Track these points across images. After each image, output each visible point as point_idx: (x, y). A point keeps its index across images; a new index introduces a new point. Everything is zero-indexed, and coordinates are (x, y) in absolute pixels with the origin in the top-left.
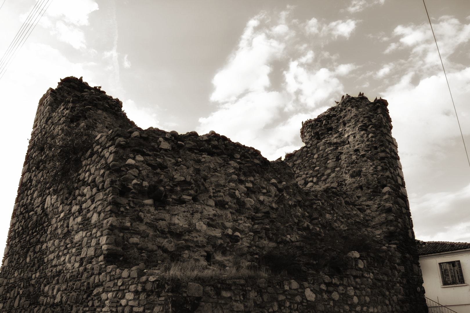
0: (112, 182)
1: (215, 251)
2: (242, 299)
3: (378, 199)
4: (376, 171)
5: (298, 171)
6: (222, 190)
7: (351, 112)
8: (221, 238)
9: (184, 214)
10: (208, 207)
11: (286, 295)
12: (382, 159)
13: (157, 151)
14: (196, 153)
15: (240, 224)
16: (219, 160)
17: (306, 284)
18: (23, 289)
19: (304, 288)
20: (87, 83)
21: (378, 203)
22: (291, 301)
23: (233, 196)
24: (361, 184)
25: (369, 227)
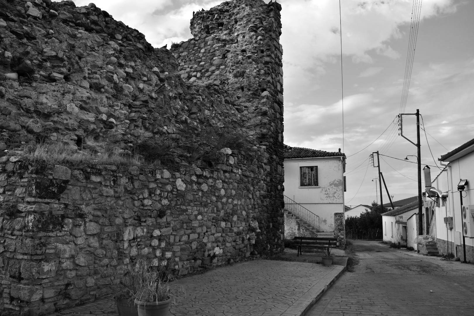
2: (113, 184)
3: (256, 101)
4: (259, 74)
5: (183, 64)
6: (98, 72)
7: (244, 11)
8: (94, 123)
9: (54, 93)
10: (82, 89)
11: (157, 183)
12: (267, 63)
13: (24, 18)
14: (71, 26)
15: (115, 110)
16: (98, 38)
17: (178, 174)
19: (176, 178)
21: (256, 105)
22: (162, 189)
23: (110, 80)
24: (242, 85)
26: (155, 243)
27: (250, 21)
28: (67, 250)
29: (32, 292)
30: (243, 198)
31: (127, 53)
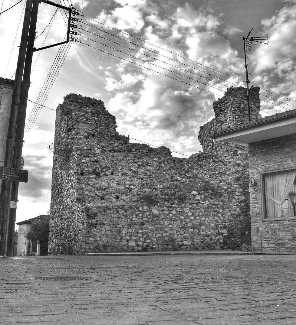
0: (77, 170)
1: (122, 195)
3: (235, 158)
8: (124, 189)
14: (113, 152)
15: (133, 182)
16: (123, 154)
17: (153, 207)
20: (80, 95)
23: (130, 170)
26: (140, 235)
27: (232, 107)
28: (98, 234)
29: (86, 245)
30: (211, 216)
31: (138, 156)
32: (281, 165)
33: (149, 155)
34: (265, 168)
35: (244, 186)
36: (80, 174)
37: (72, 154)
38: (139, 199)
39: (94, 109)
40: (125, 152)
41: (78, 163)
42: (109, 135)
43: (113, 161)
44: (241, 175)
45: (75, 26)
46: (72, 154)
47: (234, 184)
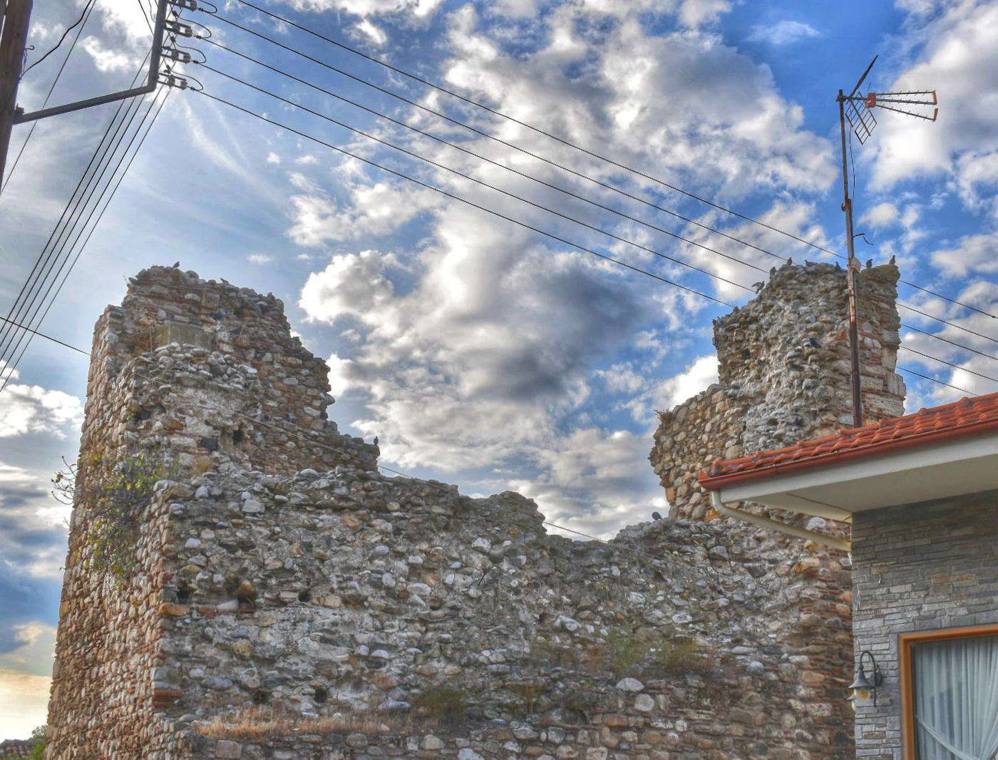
0: (166, 579)
7: (783, 315)
8: (347, 662)
13: (240, 518)
14: (310, 512)
15: (388, 635)
16: (352, 520)
17: (461, 741)
18: (79, 748)
19: (458, 749)
20: (192, 275)
21: (795, 554)
23: (377, 585)
25: (761, 612)
27: (789, 342)
31: (410, 531)
32: (983, 608)
33: (455, 524)
34: (915, 614)
35: (828, 663)
36: (175, 595)
37: (146, 514)
38: (407, 705)
39: (245, 332)
40: (361, 512)
41: (168, 550)
42: (300, 436)
43: (308, 547)
44: (818, 616)
45: (182, 30)
46: (146, 514)
47: (790, 653)
